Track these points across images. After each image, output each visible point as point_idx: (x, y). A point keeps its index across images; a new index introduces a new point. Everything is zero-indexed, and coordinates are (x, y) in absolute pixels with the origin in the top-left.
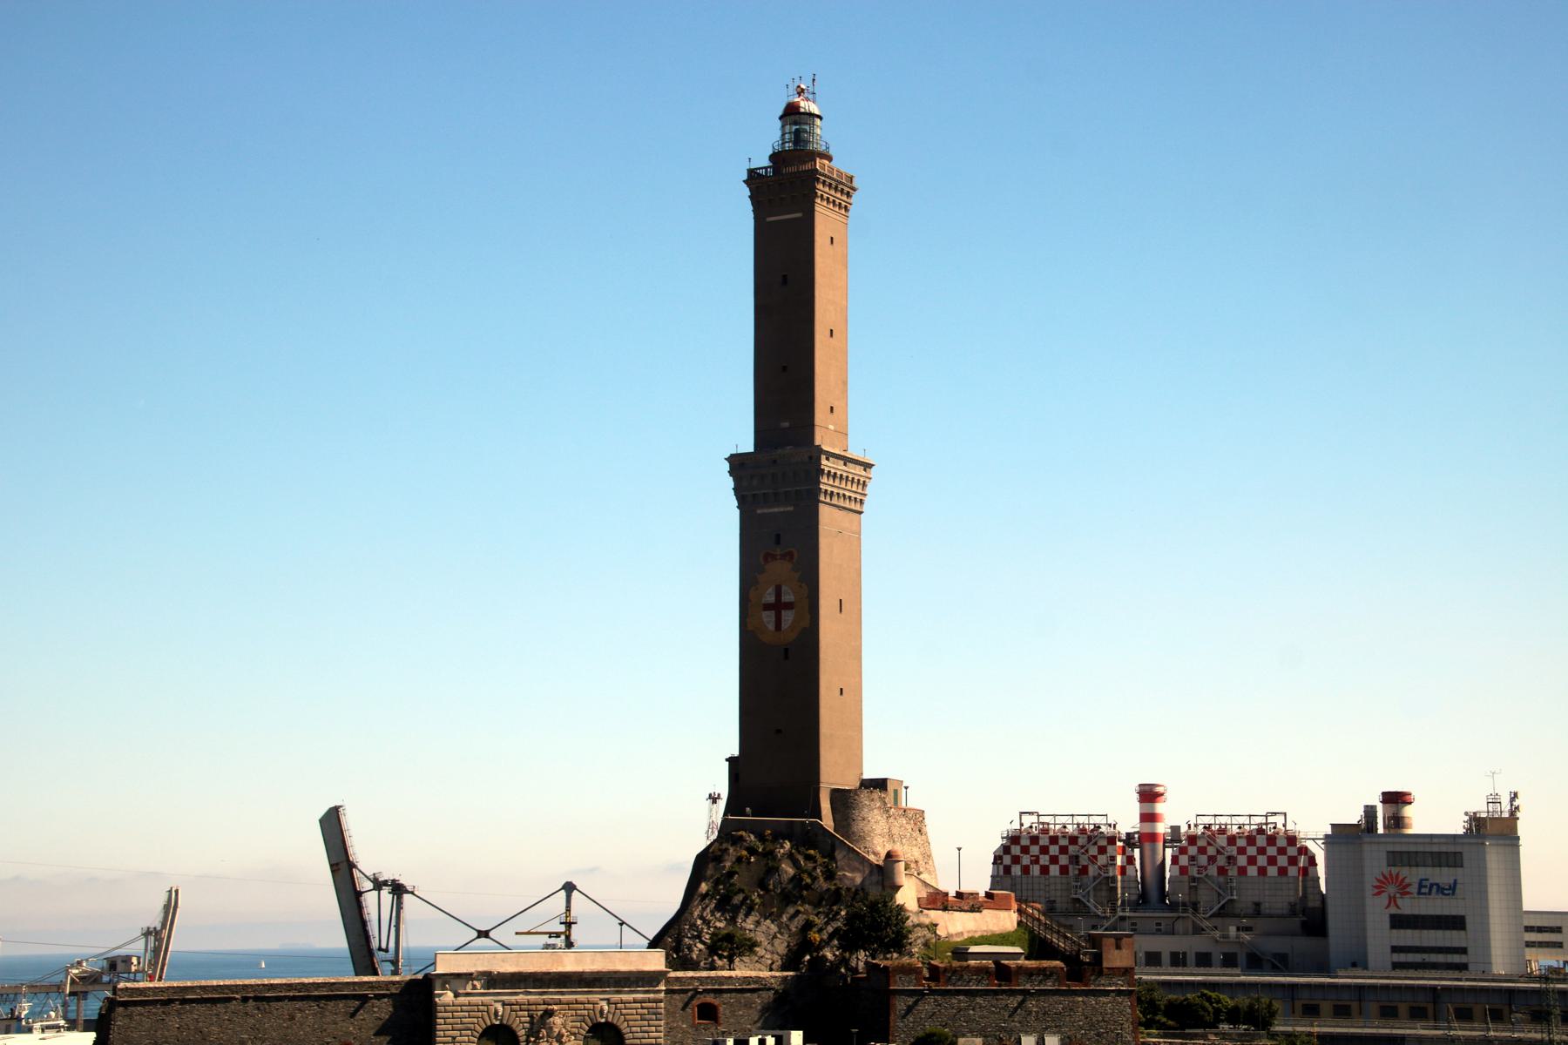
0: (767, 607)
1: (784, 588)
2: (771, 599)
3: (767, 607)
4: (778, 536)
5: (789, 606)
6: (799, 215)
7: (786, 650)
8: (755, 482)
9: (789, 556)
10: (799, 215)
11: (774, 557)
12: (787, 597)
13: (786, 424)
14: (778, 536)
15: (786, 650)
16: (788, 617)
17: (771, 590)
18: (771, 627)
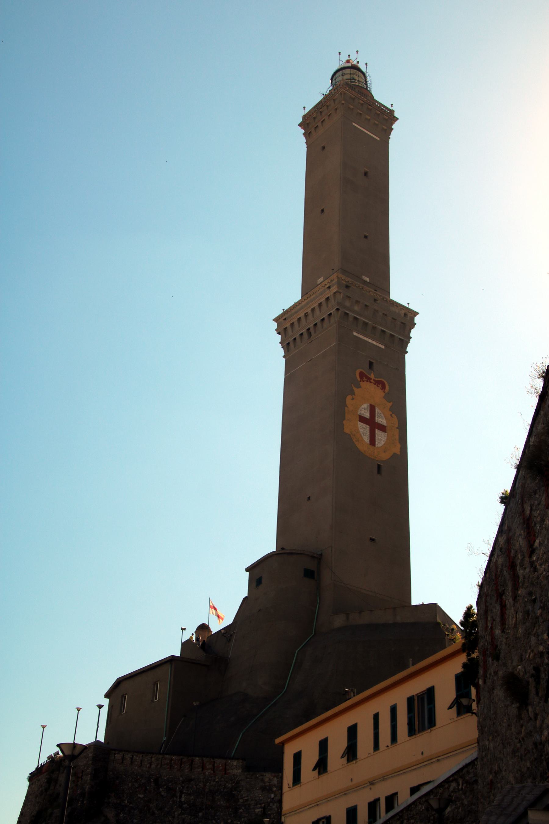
0: (362, 419)
1: (377, 410)
2: (367, 415)
3: (362, 419)
4: (371, 364)
5: (383, 428)
6: (378, 139)
7: (379, 467)
8: (356, 308)
9: (381, 384)
10: (378, 139)
11: (369, 379)
12: (381, 420)
13: (368, 280)
14: (371, 364)
15: (379, 467)
16: (381, 438)
17: (365, 406)
18: (366, 439)
